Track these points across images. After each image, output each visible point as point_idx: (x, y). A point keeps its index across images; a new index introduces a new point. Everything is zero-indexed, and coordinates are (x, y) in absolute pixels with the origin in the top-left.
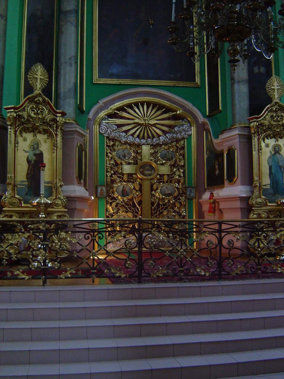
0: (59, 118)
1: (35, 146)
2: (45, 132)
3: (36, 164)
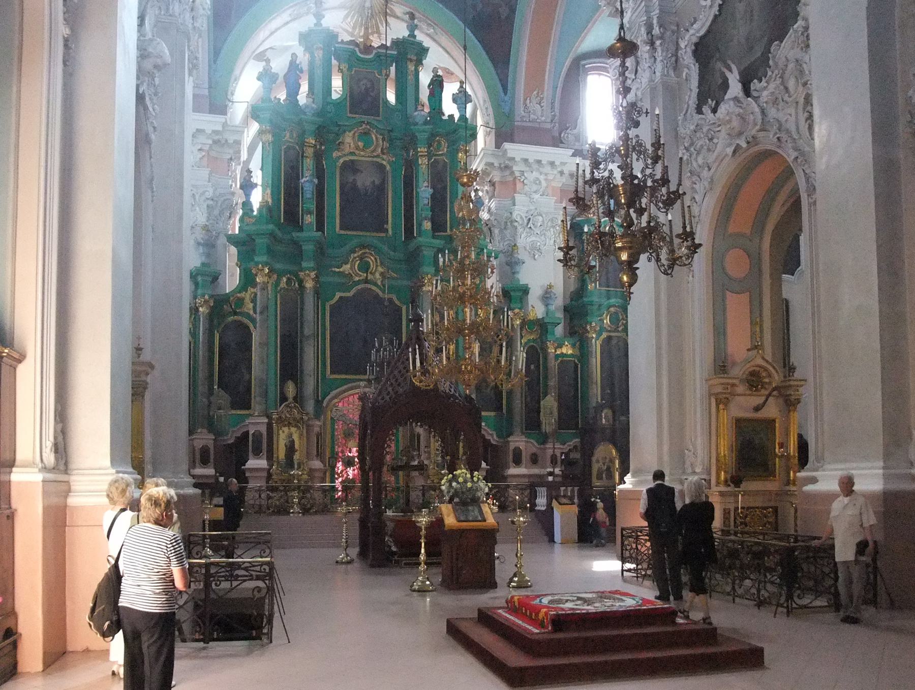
0: (305, 418)
1: (290, 435)
2: (296, 426)
3: (291, 449)
